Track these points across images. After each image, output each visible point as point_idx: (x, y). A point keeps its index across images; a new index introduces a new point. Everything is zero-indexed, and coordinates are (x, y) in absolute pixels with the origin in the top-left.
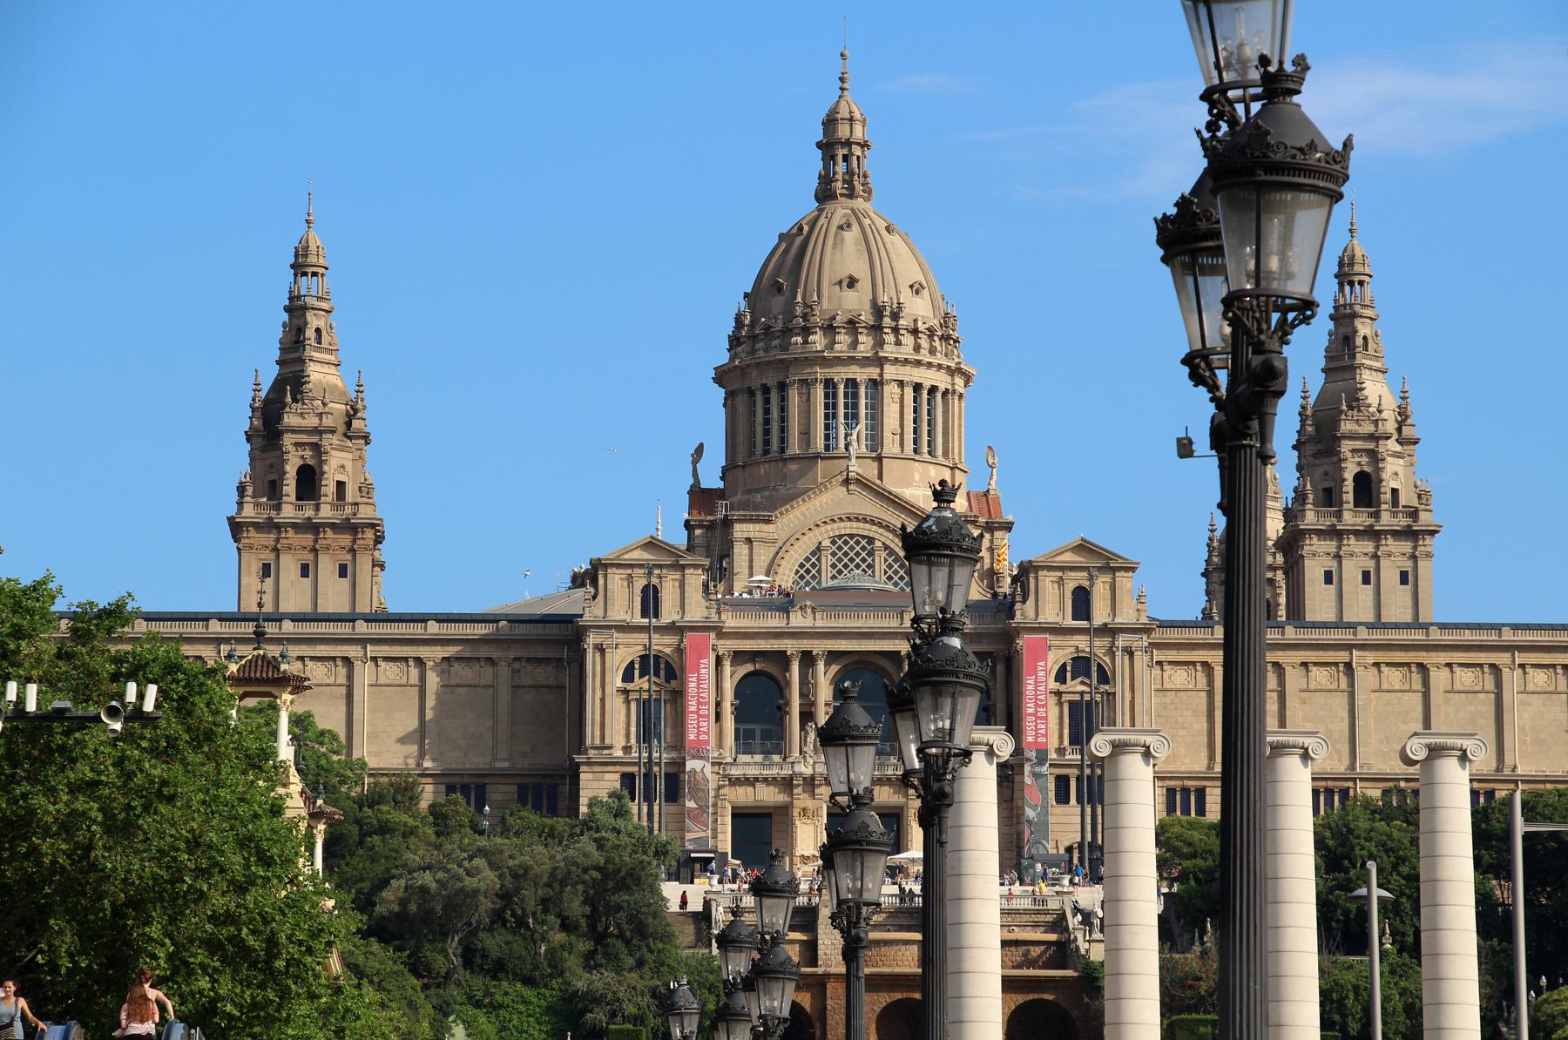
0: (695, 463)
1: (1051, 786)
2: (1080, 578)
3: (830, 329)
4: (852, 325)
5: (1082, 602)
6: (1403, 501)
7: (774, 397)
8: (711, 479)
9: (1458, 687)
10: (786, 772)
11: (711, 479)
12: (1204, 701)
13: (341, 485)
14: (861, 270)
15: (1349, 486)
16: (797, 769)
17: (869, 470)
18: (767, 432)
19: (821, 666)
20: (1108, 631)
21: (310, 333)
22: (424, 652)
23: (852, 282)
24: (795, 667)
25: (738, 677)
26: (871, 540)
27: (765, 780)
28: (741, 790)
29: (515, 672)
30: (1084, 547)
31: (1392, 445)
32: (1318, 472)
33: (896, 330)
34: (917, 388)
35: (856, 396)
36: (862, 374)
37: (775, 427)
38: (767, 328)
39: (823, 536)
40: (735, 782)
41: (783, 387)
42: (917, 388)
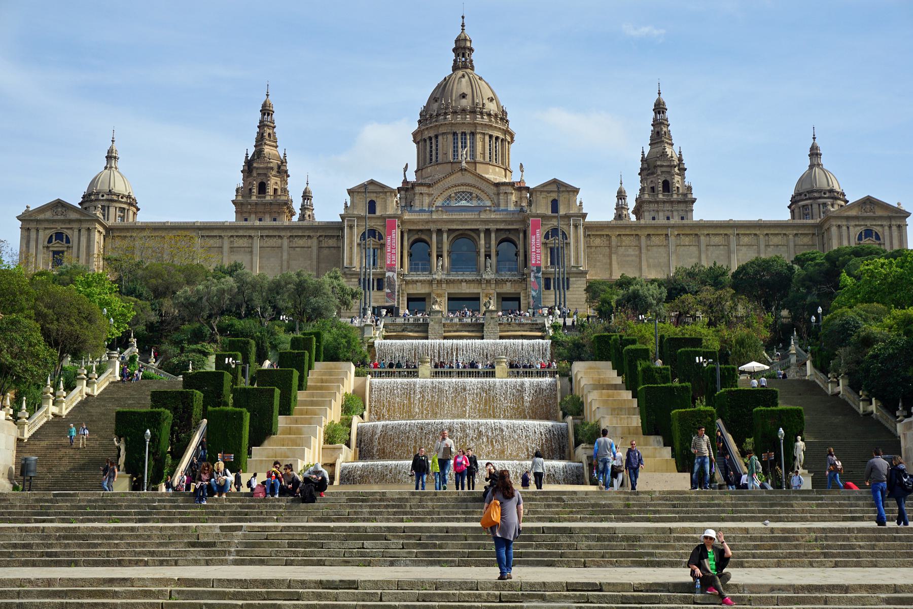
0: (405, 171)
1: (542, 282)
2: (554, 196)
3: (455, 113)
4: (464, 111)
5: (555, 205)
6: (681, 191)
7: (433, 141)
8: (412, 178)
9: (712, 243)
10: (430, 278)
11: (412, 178)
12: (608, 250)
13: (275, 190)
14: (468, 91)
15: (661, 185)
16: (434, 276)
17: (471, 168)
18: (431, 156)
19: (445, 236)
20: (567, 217)
21: (266, 135)
22: (282, 234)
23: (464, 96)
24: (434, 236)
25: (411, 241)
26: (471, 194)
27: (421, 281)
28: (410, 286)
29: (320, 241)
30: (555, 182)
31: (676, 169)
32: (649, 181)
33: (482, 113)
34: (491, 136)
35: (465, 139)
36: (468, 131)
37: (434, 153)
38: (431, 115)
39: (452, 192)
40: (407, 283)
41: (436, 137)
42: (491, 136)
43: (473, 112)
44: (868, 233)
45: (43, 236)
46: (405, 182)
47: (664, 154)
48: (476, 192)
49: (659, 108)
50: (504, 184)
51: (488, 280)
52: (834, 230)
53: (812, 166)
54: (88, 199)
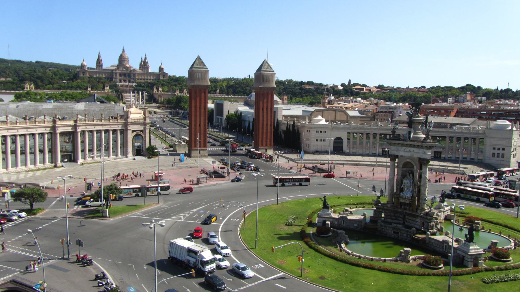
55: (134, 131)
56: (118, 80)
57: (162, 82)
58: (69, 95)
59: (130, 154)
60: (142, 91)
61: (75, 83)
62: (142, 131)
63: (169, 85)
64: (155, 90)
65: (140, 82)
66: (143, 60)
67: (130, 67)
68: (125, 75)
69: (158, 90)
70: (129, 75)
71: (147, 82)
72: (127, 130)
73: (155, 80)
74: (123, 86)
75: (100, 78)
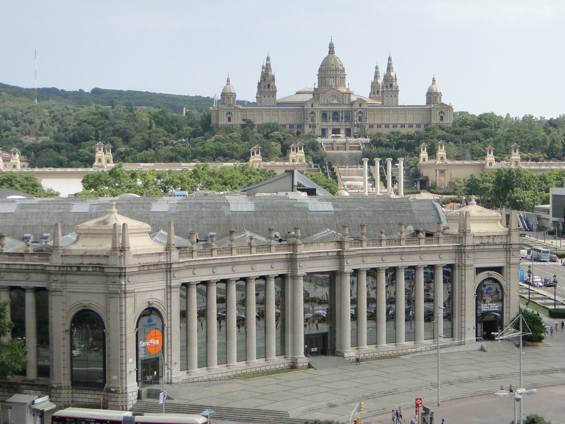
5: (360, 105)
8: (316, 87)
11: (316, 87)
14: (334, 64)
43: (336, 70)
44: (442, 112)
45: (225, 113)
46: (315, 88)
47: (390, 75)
48: (337, 95)
49: (390, 59)
50: (345, 93)
51: (342, 125)
52: (433, 111)
53: (433, 84)
54: (223, 95)
55: (479, 270)
56: (318, 131)
57: (440, 132)
58: (213, 174)
59: (471, 336)
60: (383, 156)
61: (210, 144)
62: (499, 270)
63: (458, 138)
64: (424, 154)
65: (379, 135)
66: (383, 72)
67: (350, 94)
68: (336, 116)
69: (432, 153)
70: (347, 115)
71: (398, 133)
72: (462, 266)
73: (418, 126)
74: (331, 146)
75: (274, 127)
